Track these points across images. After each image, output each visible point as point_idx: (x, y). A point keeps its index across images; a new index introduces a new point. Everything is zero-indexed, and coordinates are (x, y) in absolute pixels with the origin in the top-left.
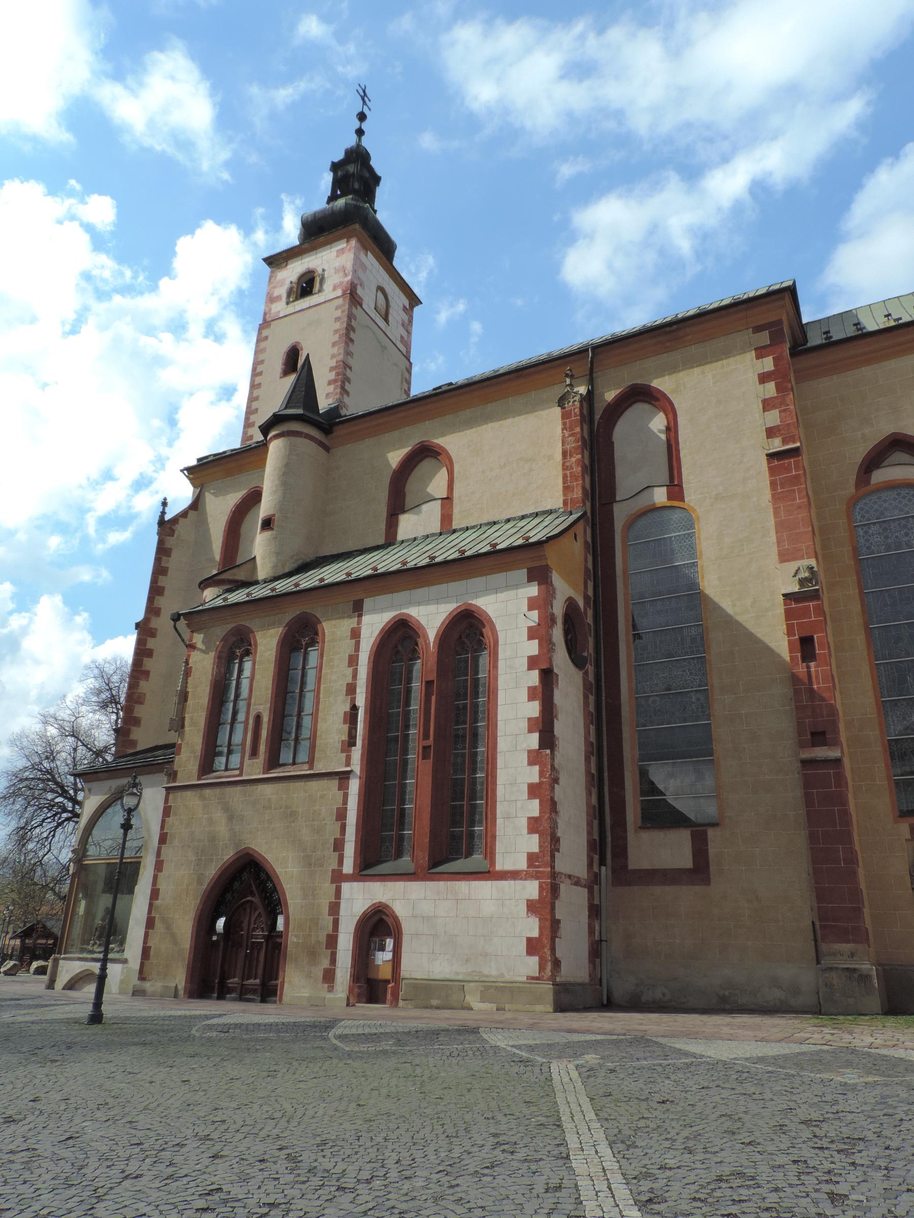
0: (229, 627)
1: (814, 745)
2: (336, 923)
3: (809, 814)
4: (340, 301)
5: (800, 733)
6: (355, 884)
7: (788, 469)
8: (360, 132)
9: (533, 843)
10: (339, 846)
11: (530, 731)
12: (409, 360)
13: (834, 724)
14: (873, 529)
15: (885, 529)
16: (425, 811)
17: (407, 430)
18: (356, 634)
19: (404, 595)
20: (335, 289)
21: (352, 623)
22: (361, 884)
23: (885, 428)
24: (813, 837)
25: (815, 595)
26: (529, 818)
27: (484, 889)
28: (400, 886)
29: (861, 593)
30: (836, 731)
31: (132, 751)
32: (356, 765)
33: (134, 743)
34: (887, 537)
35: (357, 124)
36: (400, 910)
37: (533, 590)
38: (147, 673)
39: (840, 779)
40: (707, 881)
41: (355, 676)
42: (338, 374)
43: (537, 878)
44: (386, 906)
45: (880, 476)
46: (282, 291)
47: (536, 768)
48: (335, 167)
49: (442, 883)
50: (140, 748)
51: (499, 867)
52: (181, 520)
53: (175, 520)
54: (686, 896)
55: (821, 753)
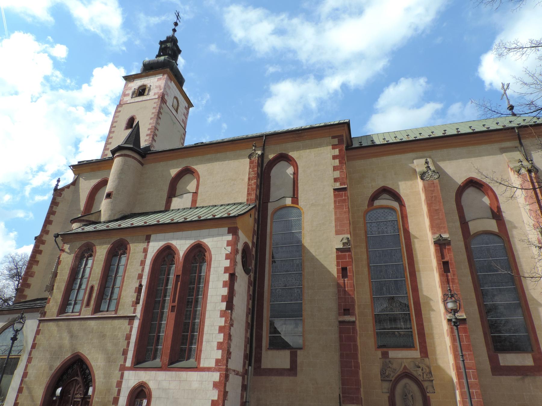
0: (83, 242)
1: (344, 315)
2: (119, 391)
3: (341, 345)
4: (157, 100)
5: (339, 309)
6: (131, 372)
7: (342, 196)
8: (174, 30)
9: (218, 354)
10: (125, 353)
11: (222, 301)
12: (185, 130)
13: (353, 306)
14: (373, 224)
15: (378, 225)
16: (169, 337)
17: (180, 160)
18: (145, 251)
19: (171, 234)
20: (155, 94)
21: (144, 245)
22: (134, 372)
23: (380, 183)
24: (342, 356)
25: (349, 250)
26: (218, 342)
27: (194, 376)
28: (153, 373)
29: (367, 251)
30: (354, 309)
31: (23, 300)
32: (138, 314)
33: (25, 296)
34: (379, 228)
35: (173, 27)
36: (152, 385)
37: (230, 237)
38: (37, 262)
39: (354, 329)
40: (295, 374)
41: (143, 270)
42: (151, 132)
43: (219, 371)
44: (145, 383)
45: (377, 203)
46: (130, 92)
47: (224, 319)
48: (161, 43)
49: (174, 373)
50: (28, 299)
51: (201, 365)
52: (66, 190)
53: (63, 189)
54: (286, 381)
55: (347, 318)
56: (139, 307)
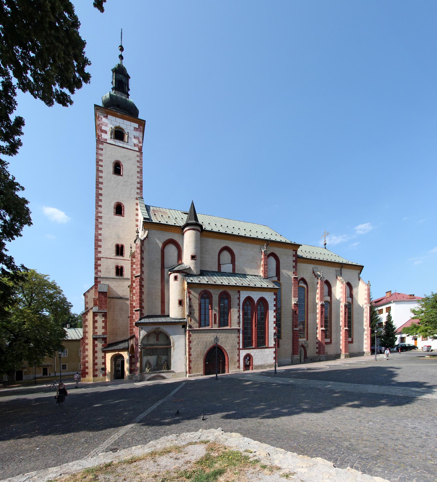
0: (203, 289)
10: (239, 343)
32: (241, 328)
56: (241, 325)
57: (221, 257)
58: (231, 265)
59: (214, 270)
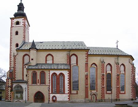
0: (33, 71)
17: (48, 52)
18: (49, 74)
45: (92, 66)
57: (48, 58)
58: (52, 61)
59: (44, 63)
